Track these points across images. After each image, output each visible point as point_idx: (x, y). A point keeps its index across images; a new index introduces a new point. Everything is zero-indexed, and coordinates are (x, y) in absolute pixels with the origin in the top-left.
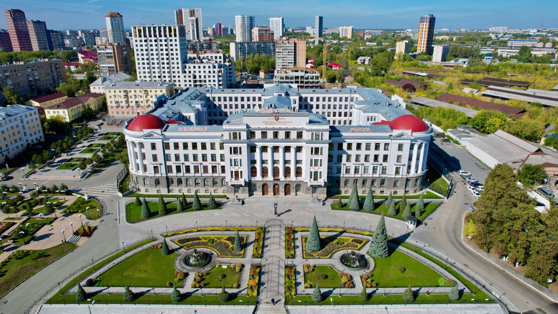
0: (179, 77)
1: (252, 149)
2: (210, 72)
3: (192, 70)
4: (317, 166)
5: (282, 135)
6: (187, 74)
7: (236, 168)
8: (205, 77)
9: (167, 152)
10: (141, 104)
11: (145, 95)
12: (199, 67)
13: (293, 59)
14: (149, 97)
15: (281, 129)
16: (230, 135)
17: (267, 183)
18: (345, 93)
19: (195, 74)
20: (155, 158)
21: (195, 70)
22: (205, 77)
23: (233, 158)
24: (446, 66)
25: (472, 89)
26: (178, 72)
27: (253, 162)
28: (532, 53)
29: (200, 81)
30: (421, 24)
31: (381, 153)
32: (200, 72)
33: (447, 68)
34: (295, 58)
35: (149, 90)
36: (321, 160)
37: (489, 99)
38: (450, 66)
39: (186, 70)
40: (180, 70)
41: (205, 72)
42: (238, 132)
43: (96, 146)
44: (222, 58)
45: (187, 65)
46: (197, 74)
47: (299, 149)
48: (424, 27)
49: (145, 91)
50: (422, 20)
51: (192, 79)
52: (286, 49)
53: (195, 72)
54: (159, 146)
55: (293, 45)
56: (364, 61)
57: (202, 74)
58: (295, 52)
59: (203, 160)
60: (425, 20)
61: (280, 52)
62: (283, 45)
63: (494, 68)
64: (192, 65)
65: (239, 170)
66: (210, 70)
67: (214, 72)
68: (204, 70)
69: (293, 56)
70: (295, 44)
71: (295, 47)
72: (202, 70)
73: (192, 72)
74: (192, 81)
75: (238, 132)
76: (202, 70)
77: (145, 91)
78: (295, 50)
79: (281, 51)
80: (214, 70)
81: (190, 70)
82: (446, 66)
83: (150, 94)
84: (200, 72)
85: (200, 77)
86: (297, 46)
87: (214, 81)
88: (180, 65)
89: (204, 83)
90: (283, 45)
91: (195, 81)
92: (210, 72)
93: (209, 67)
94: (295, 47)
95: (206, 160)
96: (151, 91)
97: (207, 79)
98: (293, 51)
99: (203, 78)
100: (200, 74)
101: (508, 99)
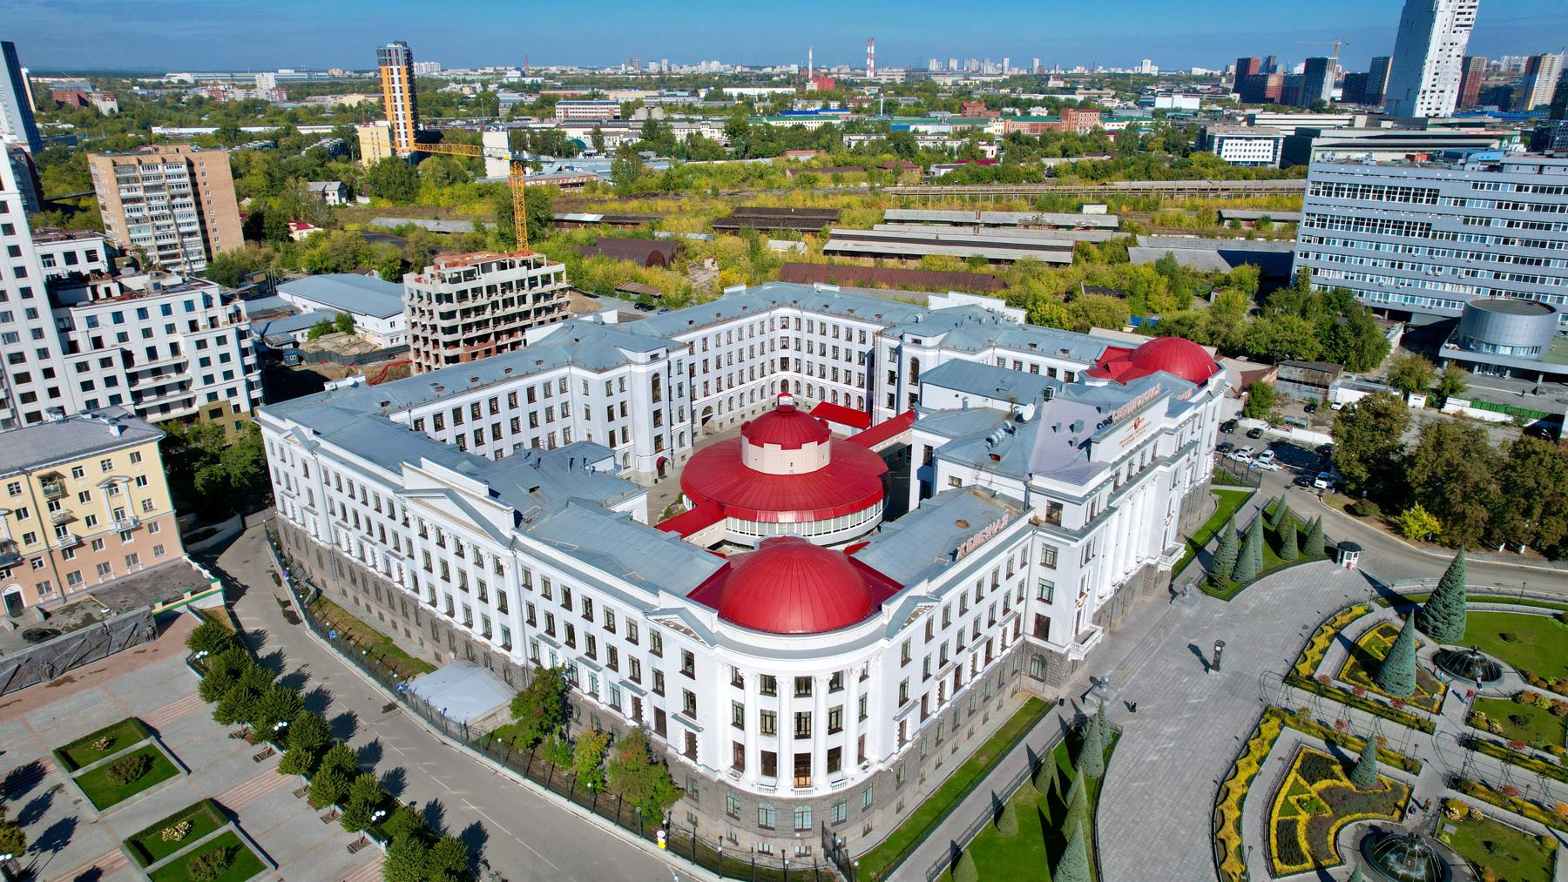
0: (49, 373)
2: (193, 326)
3: (108, 332)
6: (86, 351)
8: (174, 348)
10: (25, 550)
11: (43, 501)
12: (143, 313)
13: (195, 219)
14: (69, 504)
18: (760, 311)
19: (127, 346)
21: (120, 328)
22: (174, 348)
24: (563, 186)
25: (791, 243)
26: (43, 353)
28: (676, 132)
29: (156, 372)
30: (384, 69)
32: (147, 333)
33: (568, 190)
34: (200, 213)
35: (65, 470)
37: (869, 262)
38: (576, 185)
39: (73, 336)
40: (52, 341)
41: (170, 329)
43: (189, 835)
44: (102, 255)
45: (78, 315)
46: (138, 346)
48: (396, 76)
49: (46, 480)
50: (385, 57)
51: (118, 370)
52: (158, 188)
53: (123, 337)
55: (184, 169)
56: (324, 194)
57: (161, 342)
58: (197, 195)
60: (394, 57)
61: (138, 200)
62: (141, 172)
63: (677, 180)
64: (104, 312)
66: (192, 316)
67: (213, 322)
68: (169, 320)
69: (193, 209)
70: (190, 165)
71: (192, 175)
72: (156, 321)
73: (109, 339)
74: (122, 380)
76: (156, 321)
77: (46, 480)
78: (195, 185)
79: (140, 193)
80: (211, 313)
81: (95, 333)
82: (563, 186)
83: (73, 486)
84: (147, 333)
85: (152, 353)
86: (197, 169)
87: (225, 358)
88: (46, 320)
89: (175, 378)
90: (141, 172)
91: (133, 378)
92: (193, 326)
93: (189, 306)
94: (192, 175)
96: (78, 472)
97: (189, 352)
98: (189, 189)
99: (165, 358)
100: (149, 343)
101: (919, 257)
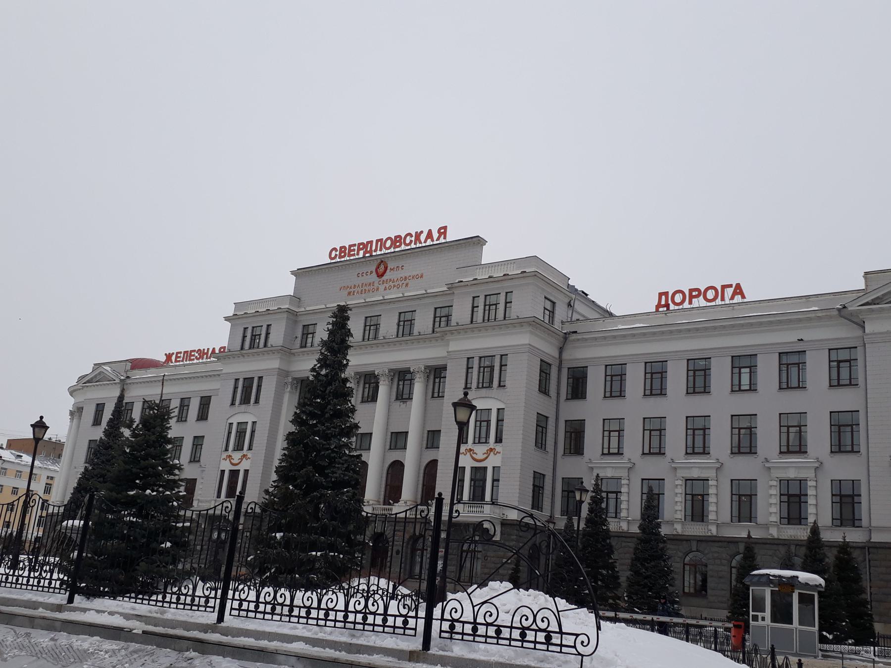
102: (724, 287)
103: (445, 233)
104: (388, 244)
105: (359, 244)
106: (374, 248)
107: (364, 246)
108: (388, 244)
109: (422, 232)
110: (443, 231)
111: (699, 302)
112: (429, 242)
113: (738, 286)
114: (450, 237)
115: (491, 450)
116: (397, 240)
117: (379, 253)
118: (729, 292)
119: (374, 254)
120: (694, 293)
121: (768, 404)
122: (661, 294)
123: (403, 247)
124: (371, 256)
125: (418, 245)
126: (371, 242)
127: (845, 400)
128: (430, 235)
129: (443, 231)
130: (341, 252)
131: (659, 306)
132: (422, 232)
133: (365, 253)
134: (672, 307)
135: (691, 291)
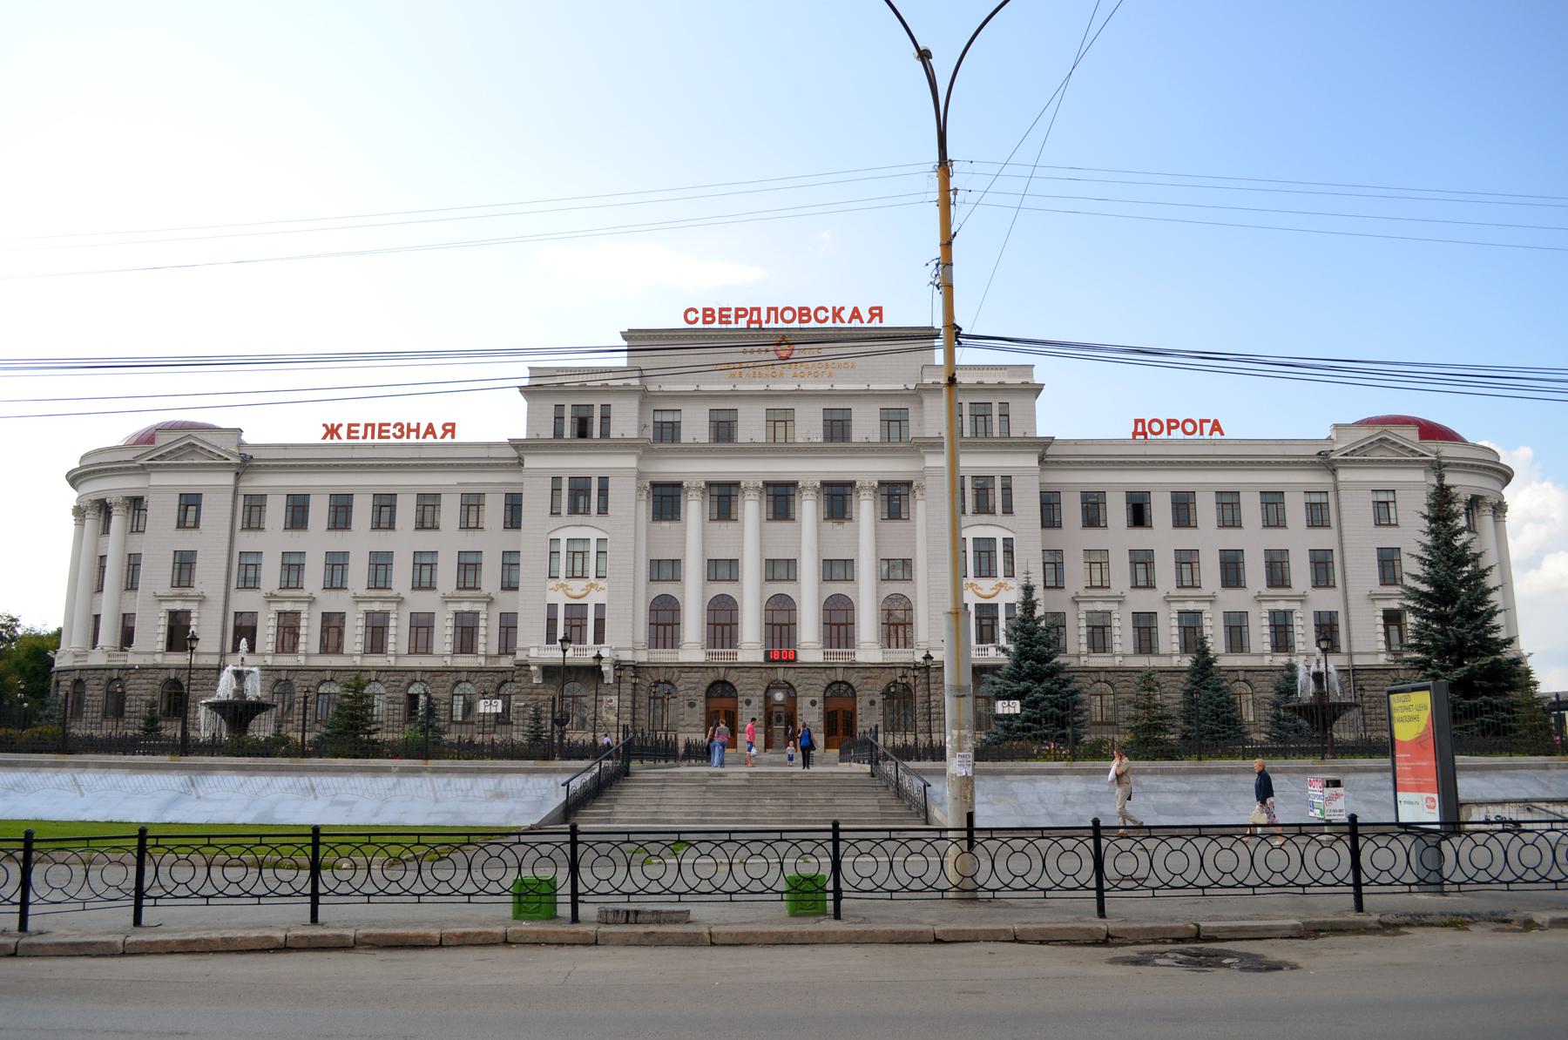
1: (666, 500)
4: (991, 574)
5: (809, 424)
7: (577, 586)
9: (247, 541)
15: (799, 395)
16: (559, 419)
17: (732, 677)
20: (184, 564)
23: (564, 535)
27: (665, 569)
31: (1298, 540)
36: (1008, 543)
42: (597, 403)
47: (895, 498)
54: (217, 512)
59: (418, 586)
65: (591, 600)
75: (597, 403)
95: (431, 587)
102: (1202, 421)
103: (880, 315)
104: (788, 315)
105: (737, 310)
106: (764, 317)
107: (740, 312)
108: (788, 315)
109: (842, 308)
110: (876, 312)
111: (1177, 434)
112: (856, 323)
113: (1216, 422)
114: (888, 322)
115: (1001, 585)
116: (803, 313)
117: (772, 325)
118: (1207, 427)
119: (765, 326)
120: (1172, 424)
121: (1253, 540)
122: (1137, 421)
123: (813, 324)
124: (761, 329)
125: (839, 324)
126: (759, 310)
127: (1323, 539)
128: (856, 314)
129: (876, 312)
130: (705, 316)
131: (1135, 433)
132: (842, 308)
133: (750, 321)
134: (1149, 436)
135: (1169, 421)
